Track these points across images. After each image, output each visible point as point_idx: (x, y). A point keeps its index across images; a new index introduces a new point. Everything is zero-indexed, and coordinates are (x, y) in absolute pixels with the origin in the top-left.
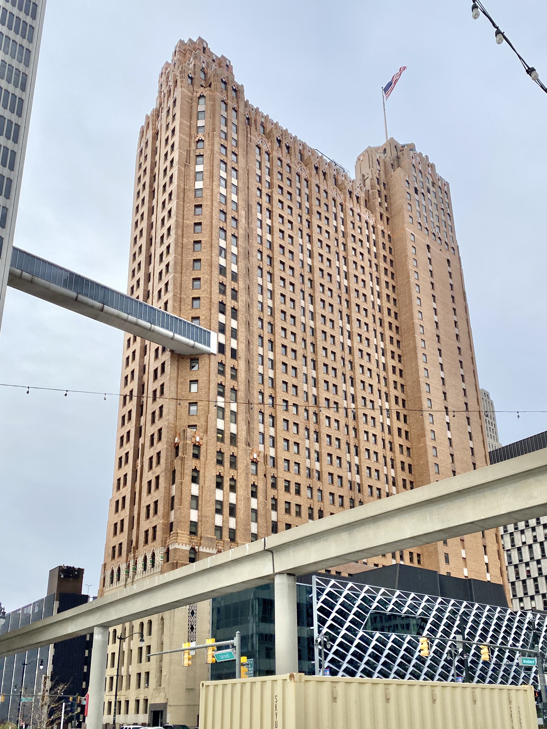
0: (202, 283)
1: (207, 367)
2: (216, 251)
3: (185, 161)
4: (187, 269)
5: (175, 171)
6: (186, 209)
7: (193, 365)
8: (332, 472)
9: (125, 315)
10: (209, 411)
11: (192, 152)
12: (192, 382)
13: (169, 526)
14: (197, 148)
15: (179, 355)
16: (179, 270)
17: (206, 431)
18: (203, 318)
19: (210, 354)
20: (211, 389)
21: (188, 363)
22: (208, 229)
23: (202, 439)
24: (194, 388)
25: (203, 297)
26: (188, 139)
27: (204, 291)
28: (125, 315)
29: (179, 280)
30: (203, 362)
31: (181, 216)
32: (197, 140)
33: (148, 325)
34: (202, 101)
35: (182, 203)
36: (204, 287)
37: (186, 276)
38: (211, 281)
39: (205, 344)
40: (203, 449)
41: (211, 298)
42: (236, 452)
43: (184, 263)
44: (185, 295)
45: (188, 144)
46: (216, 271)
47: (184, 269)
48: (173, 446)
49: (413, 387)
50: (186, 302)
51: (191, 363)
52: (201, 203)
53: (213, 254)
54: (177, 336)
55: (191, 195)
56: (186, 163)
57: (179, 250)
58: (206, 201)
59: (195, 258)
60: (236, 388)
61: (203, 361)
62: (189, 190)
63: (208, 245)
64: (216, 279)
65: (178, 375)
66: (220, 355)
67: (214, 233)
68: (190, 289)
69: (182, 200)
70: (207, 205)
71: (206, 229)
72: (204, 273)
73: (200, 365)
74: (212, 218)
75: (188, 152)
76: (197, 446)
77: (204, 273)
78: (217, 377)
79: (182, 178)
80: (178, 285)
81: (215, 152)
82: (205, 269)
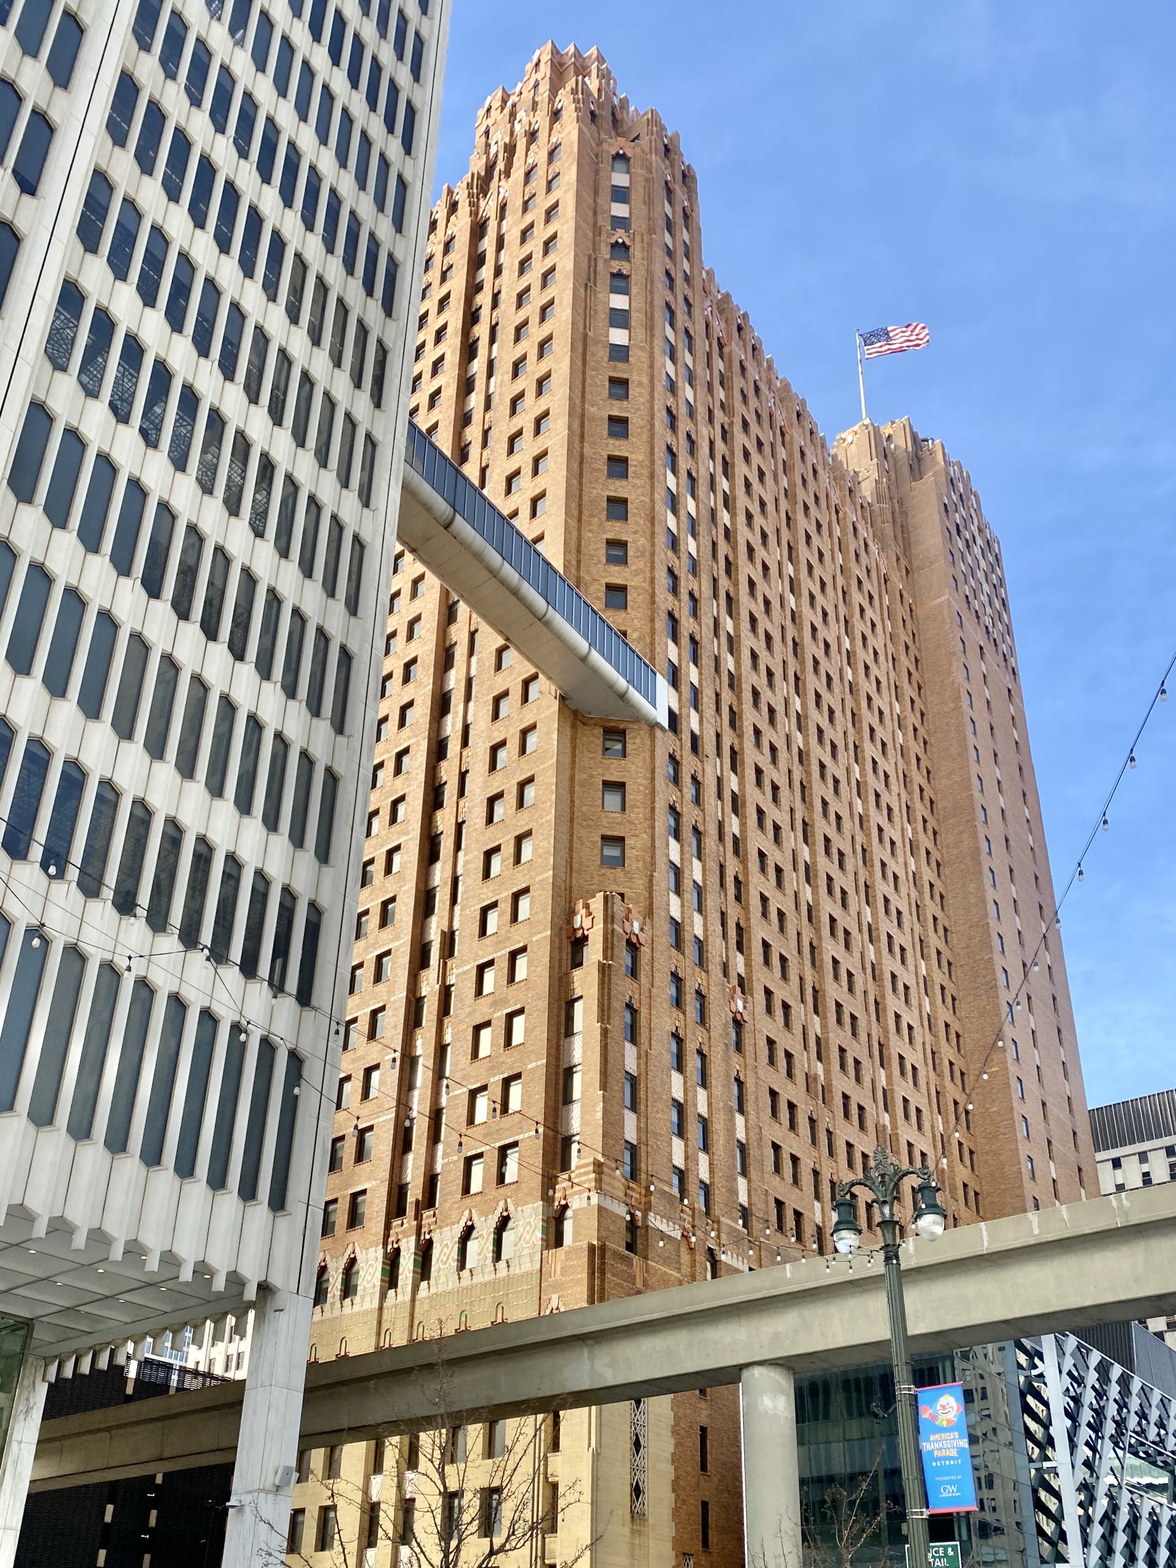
0: (630, 553)
1: (647, 755)
2: (660, 495)
3: (585, 276)
4: (592, 516)
5: (563, 290)
6: (588, 380)
7: (608, 744)
8: (848, 1093)
9: (495, 558)
10: (653, 864)
11: (600, 266)
12: (608, 785)
13: (559, 1145)
14: (612, 258)
15: (575, 713)
16: (576, 513)
17: (649, 913)
18: (635, 635)
19: (654, 726)
20: (657, 811)
21: (595, 737)
22: (645, 437)
23: (642, 930)
24: (613, 800)
25: (635, 588)
26: (590, 234)
27: (637, 573)
28: (495, 558)
29: (575, 533)
30: (638, 741)
31: (578, 392)
32: (613, 241)
33: (540, 603)
34: (620, 165)
35: (580, 363)
36: (636, 562)
37: (590, 531)
38: (653, 555)
39: (646, 697)
40: (645, 952)
41: (653, 595)
42: (705, 983)
43: (585, 498)
44: (588, 572)
45: (590, 245)
46: (662, 540)
47: (586, 512)
48: (564, 937)
49: (971, 938)
50: (592, 589)
51: (605, 739)
52: (625, 376)
53: (656, 495)
54: (596, 658)
55: (603, 354)
56: (586, 282)
57: (576, 466)
58: (639, 375)
59: (612, 494)
60: (701, 828)
61: (636, 741)
62: (596, 343)
63: (645, 472)
64: (662, 555)
65: (573, 762)
66: (671, 734)
67: (656, 450)
68: (599, 562)
69: (580, 357)
70: (640, 384)
71: (639, 434)
72: (636, 533)
73: (629, 747)
74: (652, 416)
75: (593, 261)
76: (633, 947)
77: (636, 533)
78: (667, 786)
79: (581, 311)
80: (573, 544)
81: (656, 278)
82: (637, 523)
